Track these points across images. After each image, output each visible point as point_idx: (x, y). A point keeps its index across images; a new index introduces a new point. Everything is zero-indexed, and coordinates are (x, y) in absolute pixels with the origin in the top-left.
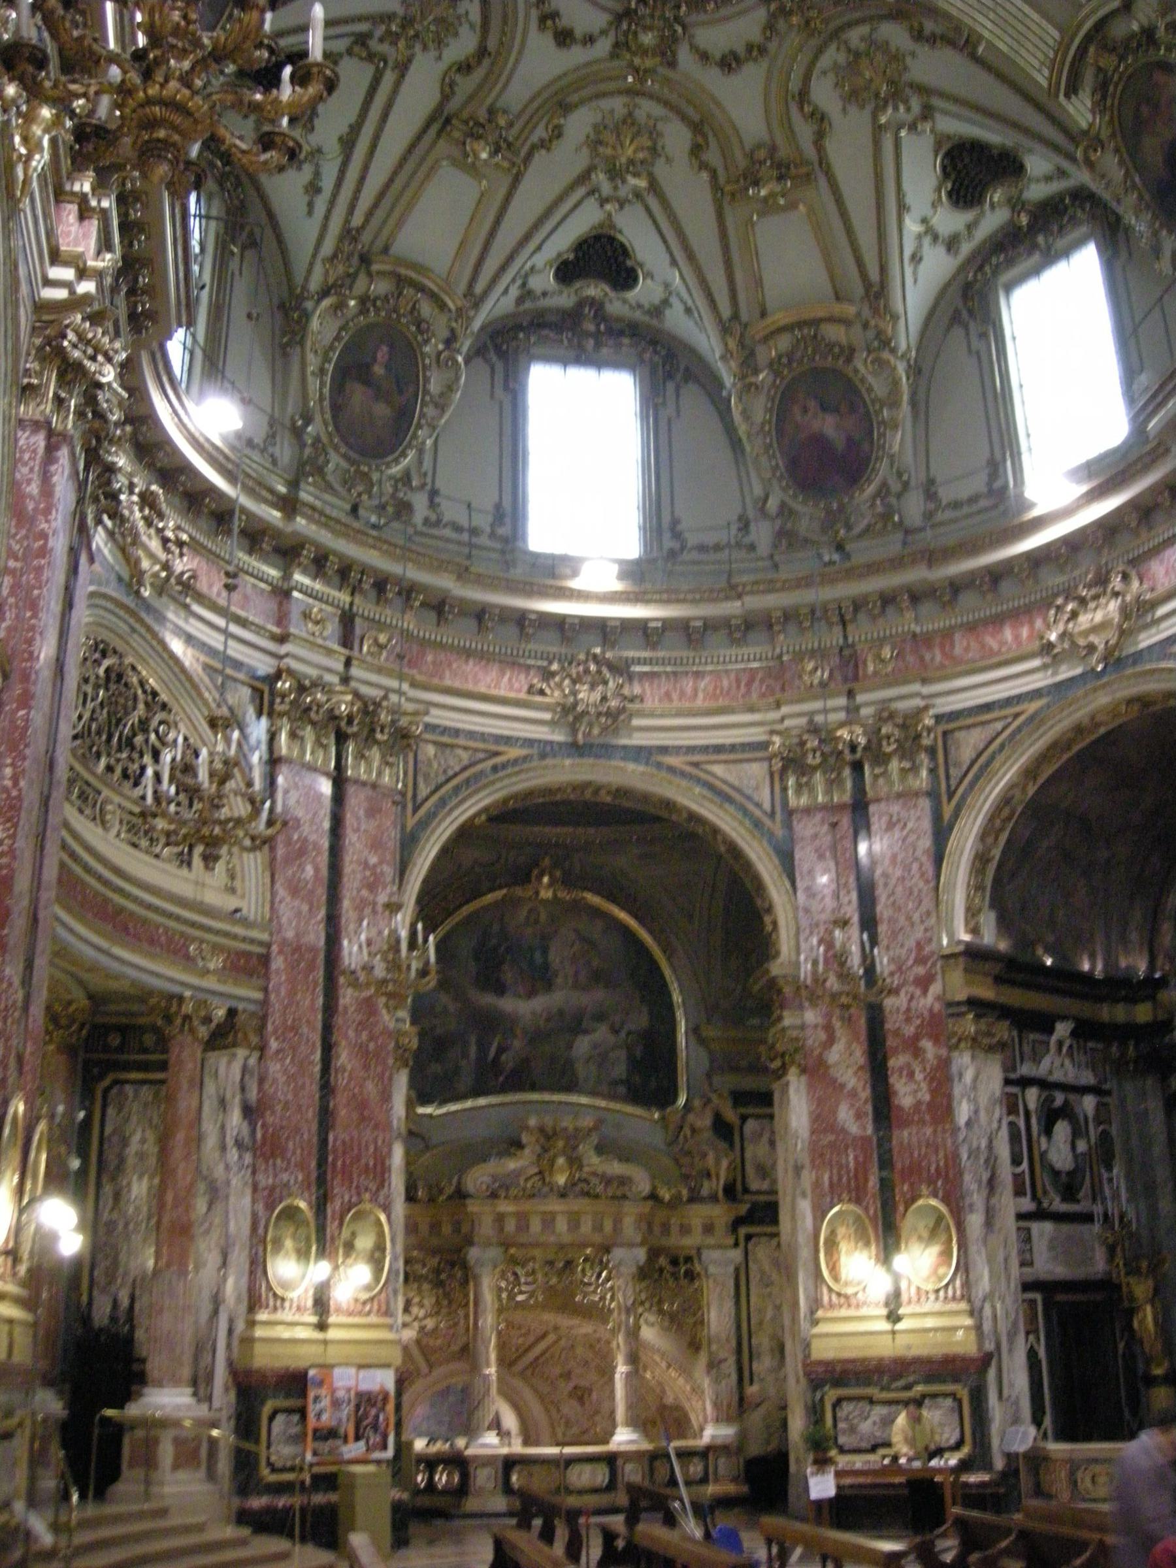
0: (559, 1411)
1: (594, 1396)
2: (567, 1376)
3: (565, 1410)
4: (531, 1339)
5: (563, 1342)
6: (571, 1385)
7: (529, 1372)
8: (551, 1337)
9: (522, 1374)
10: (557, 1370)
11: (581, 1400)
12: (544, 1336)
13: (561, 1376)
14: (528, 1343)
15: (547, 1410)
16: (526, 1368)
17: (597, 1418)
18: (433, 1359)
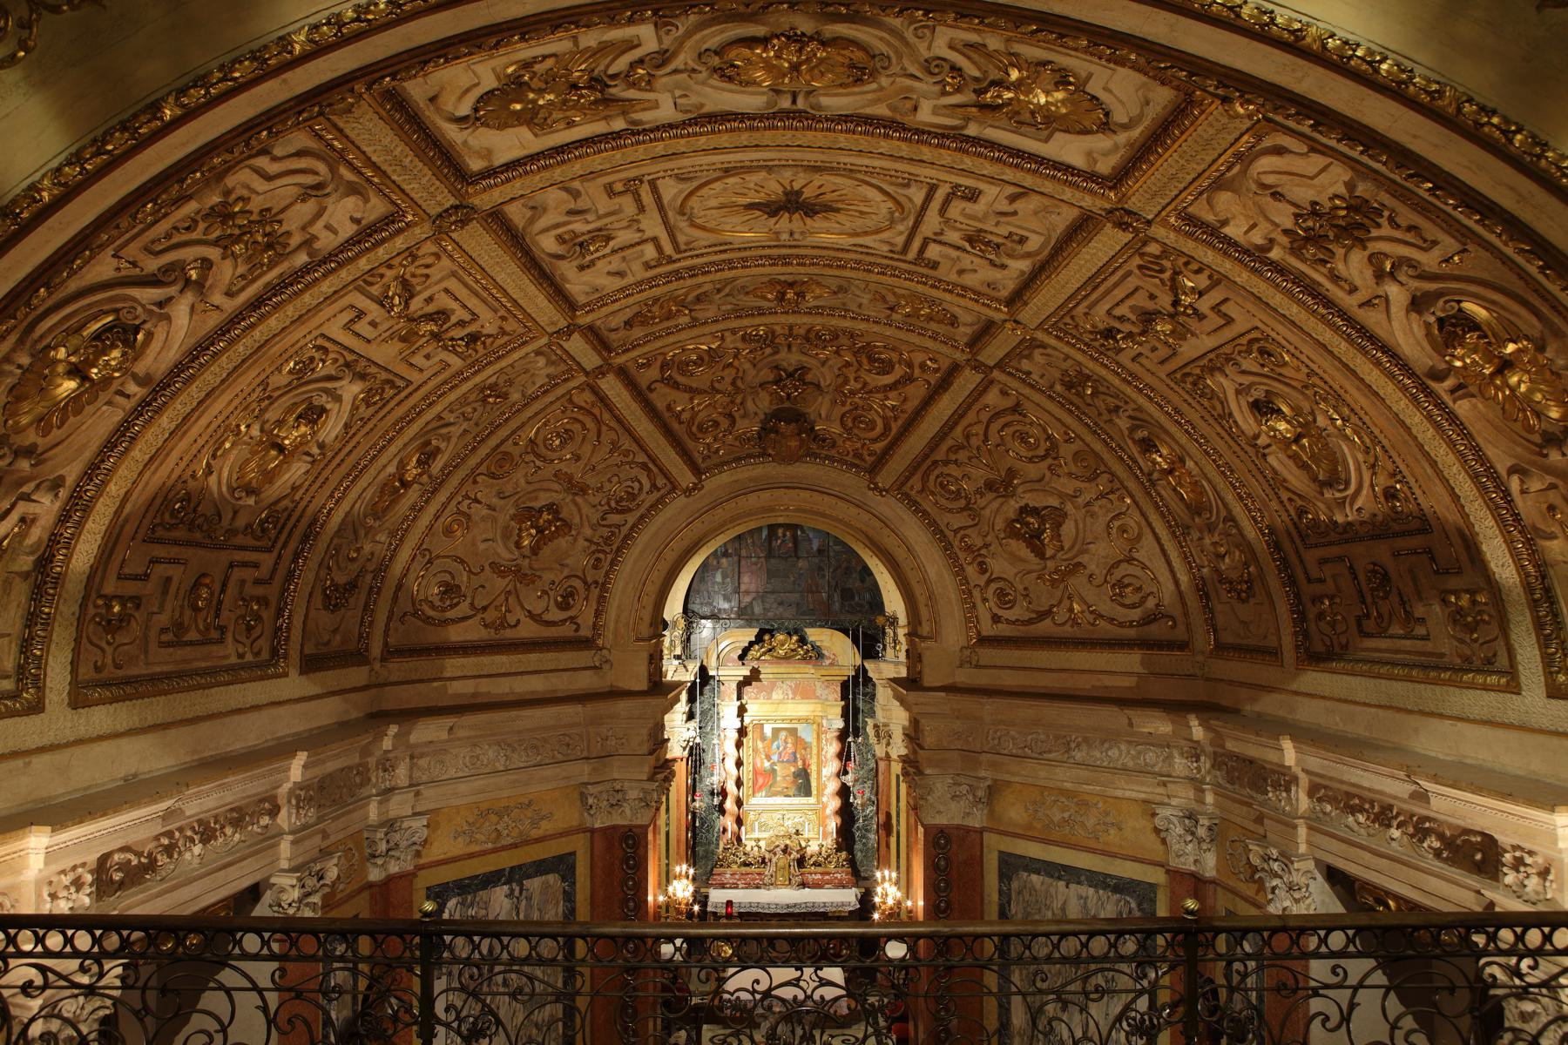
0: (983, 569)
1: (1068, 529)
2: (1002, 486)
3: (999, 566)
4: (916, 392)
5: (992, 398)
6: (1013, 506)
7: (916, 482)
8: (968, 380)
9: (900, 489)
10: (980, 475)
11: (1034, 541)
12: (944, 384)
13: (990, 486)
14: (911, 406)
15: (959, 572)
16: (913, 469)
17: (1077, 583)
18: (698, 449)
